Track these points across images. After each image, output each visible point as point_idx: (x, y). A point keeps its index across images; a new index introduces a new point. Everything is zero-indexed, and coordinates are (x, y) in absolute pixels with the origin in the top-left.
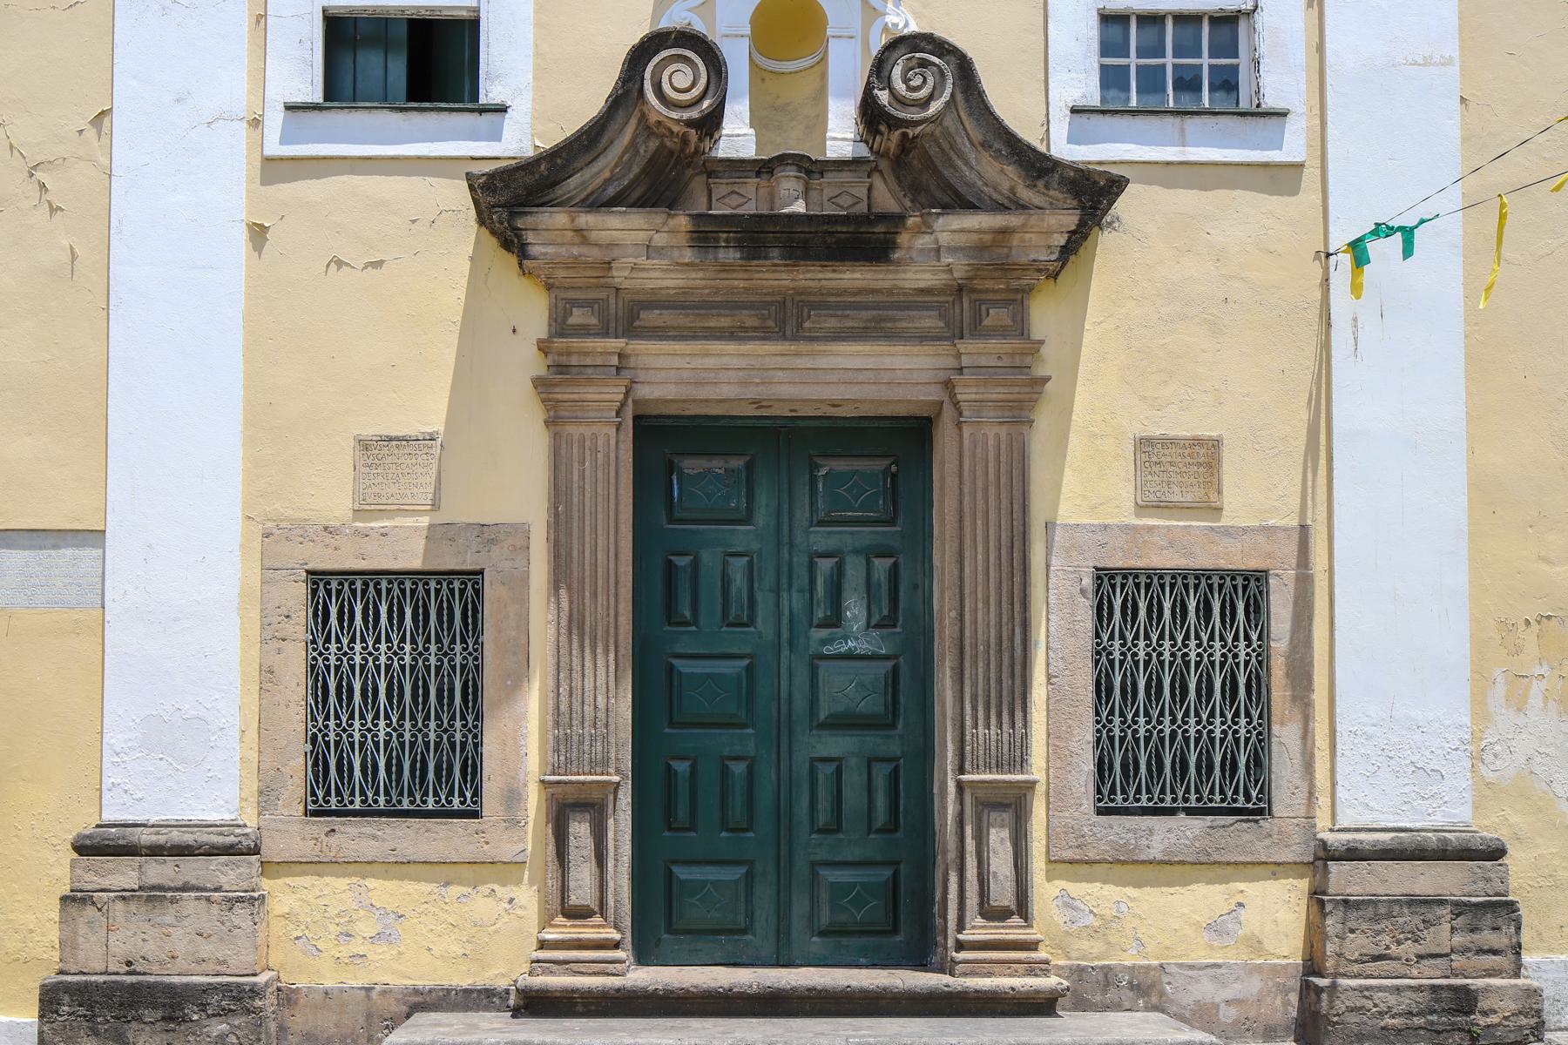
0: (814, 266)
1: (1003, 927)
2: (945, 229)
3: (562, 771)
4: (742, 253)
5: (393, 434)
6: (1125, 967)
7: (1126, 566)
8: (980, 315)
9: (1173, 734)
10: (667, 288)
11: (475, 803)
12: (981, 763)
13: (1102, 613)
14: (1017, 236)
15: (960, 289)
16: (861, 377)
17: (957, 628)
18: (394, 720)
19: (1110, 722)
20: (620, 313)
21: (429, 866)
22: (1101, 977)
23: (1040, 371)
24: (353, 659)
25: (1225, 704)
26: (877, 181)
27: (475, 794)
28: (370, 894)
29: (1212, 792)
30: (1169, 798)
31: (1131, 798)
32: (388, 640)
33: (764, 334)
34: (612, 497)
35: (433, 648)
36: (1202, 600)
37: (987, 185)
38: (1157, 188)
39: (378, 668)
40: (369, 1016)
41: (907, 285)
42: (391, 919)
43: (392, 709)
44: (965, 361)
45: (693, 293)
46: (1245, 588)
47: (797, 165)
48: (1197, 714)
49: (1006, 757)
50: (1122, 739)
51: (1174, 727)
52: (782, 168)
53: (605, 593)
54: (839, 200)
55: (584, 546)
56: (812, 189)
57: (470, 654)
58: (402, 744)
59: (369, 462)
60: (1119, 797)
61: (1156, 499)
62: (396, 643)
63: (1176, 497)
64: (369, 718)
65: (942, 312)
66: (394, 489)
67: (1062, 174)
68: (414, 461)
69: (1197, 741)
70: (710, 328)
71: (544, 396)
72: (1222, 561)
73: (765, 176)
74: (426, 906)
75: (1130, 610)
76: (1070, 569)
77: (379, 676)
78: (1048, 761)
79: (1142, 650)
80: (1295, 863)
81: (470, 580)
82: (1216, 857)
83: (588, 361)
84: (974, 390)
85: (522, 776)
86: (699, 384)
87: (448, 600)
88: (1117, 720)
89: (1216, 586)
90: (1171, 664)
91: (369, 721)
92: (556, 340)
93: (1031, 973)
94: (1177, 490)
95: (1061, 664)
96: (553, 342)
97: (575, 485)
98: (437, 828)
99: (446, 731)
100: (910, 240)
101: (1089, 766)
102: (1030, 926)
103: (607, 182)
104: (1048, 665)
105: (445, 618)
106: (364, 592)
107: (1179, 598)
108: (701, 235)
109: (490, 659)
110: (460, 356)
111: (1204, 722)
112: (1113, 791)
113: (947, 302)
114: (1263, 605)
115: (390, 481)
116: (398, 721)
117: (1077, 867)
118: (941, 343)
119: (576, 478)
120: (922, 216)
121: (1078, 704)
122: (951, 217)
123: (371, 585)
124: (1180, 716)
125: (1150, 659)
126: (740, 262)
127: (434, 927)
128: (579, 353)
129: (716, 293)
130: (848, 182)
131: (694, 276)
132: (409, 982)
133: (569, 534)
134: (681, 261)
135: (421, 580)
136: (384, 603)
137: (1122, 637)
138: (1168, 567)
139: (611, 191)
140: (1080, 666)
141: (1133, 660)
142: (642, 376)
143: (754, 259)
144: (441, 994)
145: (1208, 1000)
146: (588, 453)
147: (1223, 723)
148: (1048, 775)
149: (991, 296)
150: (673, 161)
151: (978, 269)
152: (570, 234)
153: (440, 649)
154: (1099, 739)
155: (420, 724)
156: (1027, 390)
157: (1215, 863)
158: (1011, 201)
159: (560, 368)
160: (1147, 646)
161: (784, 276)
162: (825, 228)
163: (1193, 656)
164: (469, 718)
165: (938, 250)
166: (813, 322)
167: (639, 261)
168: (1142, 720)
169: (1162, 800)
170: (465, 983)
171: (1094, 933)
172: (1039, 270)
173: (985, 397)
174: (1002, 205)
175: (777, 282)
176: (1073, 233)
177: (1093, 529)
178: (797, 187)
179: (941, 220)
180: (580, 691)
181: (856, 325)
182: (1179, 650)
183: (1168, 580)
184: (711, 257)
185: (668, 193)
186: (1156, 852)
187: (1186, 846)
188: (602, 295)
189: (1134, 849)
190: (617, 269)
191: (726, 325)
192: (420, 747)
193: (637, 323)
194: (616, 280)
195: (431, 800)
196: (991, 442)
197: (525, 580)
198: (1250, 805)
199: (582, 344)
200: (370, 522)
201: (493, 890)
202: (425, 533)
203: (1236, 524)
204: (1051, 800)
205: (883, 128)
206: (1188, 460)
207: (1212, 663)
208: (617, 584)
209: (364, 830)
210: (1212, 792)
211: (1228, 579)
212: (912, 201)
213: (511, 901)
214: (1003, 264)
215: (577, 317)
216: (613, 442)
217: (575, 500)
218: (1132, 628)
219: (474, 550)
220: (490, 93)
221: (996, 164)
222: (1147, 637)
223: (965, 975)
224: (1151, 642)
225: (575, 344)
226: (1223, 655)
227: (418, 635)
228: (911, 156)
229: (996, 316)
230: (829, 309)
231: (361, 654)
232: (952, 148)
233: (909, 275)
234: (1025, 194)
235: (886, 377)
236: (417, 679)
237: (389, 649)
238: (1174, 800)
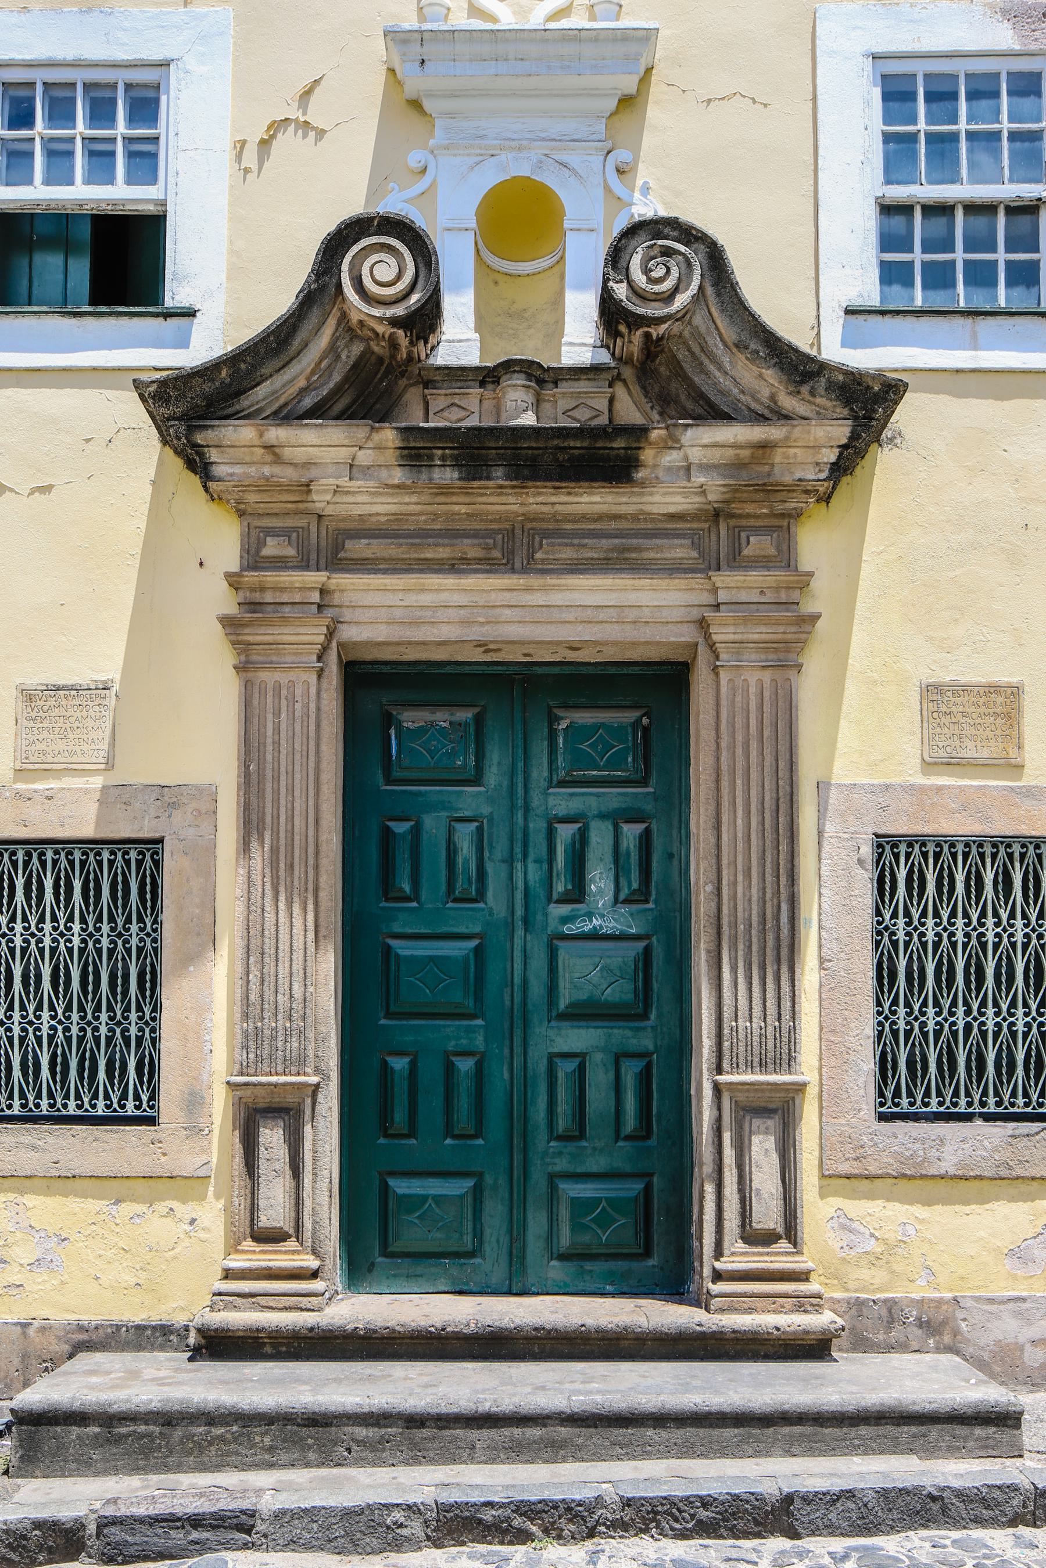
0: (546, 487)
1: (768, 1254)
2: (695, 443)
3: (252, 1071)
4: (461, 472)
5: (61, 682)
6: (913, 1300)
7: (911, 832)
8: (740, 544)
9: (968, 1027)
10: (378, 514)
11: (152, 1107)
12: (741, 1061)
13: (884, 886)
14: (779, 450)
15: (717, 514)
16: (602, 615)
17: (713, 905)
18: (60, 1012)
19: (894, 1013)
20: (323, 543)
21: (98, 1182)
22: (884, 1312)
23: (808, 607)
24: (12, 941)
25: (1029, 992)
26: (620, 390)
27: (152, 1098)
28: (29, 1213)
29: (1014, 1094)
30: (963, 1101)
31: (919, 1102)
32: (54, 918)
33: (489, 565)
34: (312, 753)
35: (105, 928)
36: (1000, 871)
37: (743, 392)
38: (944, 399)
39: (41, 951)
40: (25, 1356)
41: (655, 509)
42: (53, 1243)
43: (58, 999)
44: (722, 596)
45: (407, 520)
47: (526, 373)
48: (996, 1004)
49: (771, 1055)
50: (908, 1033)
51: (969, 1019)
52: (508, 376)
53: (303, 865)
54: (575, 413)
55: (278, 809)
56: (545, 401)
57: (148, 935)
58: (68, 1039)
59: (34, 714)
60: (905, 1101)
61: (946, 755)
62: (62, 922)
63: (969, 751)
64: (31, 1009)
65: (696, 541)
66: (61, 746)
67: (829, 378)
68: (85, 714)
69: (996, 1035)
70: (426, 559)
71: (233, 638)
72: (1024, 827)
73: (490, 386)
74: (94, 1227)
75: (916, 883)
76: (845, 836)
77: (43, 960)
78: (821, 1059)
79: (930, 929)
81: (148, 850)
82: (1019, 1171)
83: (285, 598)
84: (731, 629)
85: (205, 1077)
86: (415, 623)
87: (123, 873)
88: (902, 1011)
89: (1017, 855)
90: (965, 945)
91: (31, 1012)
92: (246, 573)
93: (800, 1309)
94: (970, 744)
95: (835, 946)
96: (243, 576)
97: (269, 741)
98: (107, 1136)
99: (119, 1024)
100: (655, 457)
101: (869, 1065)
102: (800, 1253)
103: (303, 392)
104: (820, 946)
105: (120, 894)
106: (26, 864)
107: (973, 869)
108: (413, 452)
109: (170, 940)
110: (140, 593)
111: (1004, 1014)
112: (897, 1094)
113: (703, 530)
115: (57, 736)
116: (64, 1013)
118: (694, 575)
119: (270, 732)
120: (667, 428)
121: (855, 992)
122: (701, 429)
123: (35, 855)
124: (975, 1007)
125: (940, 940)
126: (459, 483)
127: (102, 1252)
128: (274, 589)
129: (433, 520)
130: (586, 393)
131: (407, 499)
132: (72, 1317)
133: (261, 795)
134: (390, 482)
135: (92, 850)
136: (49, 874)
137: (907, 914)
138: (960, 833)
139: (308, 402)
140: (858, 948)
141: (920, 940)
142: (347, 615)
143: (474, 479)
144: (109, 1330)
145: (1011, 1340)
146: (284, 703)
147: (1026, 1015)
148: (821, 1075)
149: (752, 522)
150: (383, 369)
151: (736, 491)
152: (262, 451)
153: (113, 929)
154: (880, 1034)
155: (89, 1017)
156: (793, 629)
158: (772, 411)
159: (252, 606)
160: (937, 925)
161: (512, 499)
162: (556, 442)
163: (990, 937)
164: (146, 1010)
165: (688, 468)
166: (547, 553)
167: (340, 482)
168: (931, 1011)
169: (955, 1105)
170: (138, 1319)
171: (875, 1260)
172: (807, 492)
173: (745, 637)
174: (762, 416)
175: (503, 507)
176: (844, 447)
177: (872, 790)
178: (525, 398)
179: (690, 433)
180: (273, 978)
181: (596, 556)
182: (975, 929)
184: (424, 476)
185: (378, 406)
186: (948, 1166)
188: (300, 522)
189: (923, 1161)
190: (318, 491)
191: (445, 556)
192: (90, 1043)
193: (341, 555)
194: (318, 505)
195: (101, 1103)
196: (752, 690)
197: (211, 849)
199: (277, 579)
200: (33, 783)
201: (171, 1209)
202: (97, 795)
203: (1039, 784)
204: (824, 1104)
205: (622, 328)
206: (983, 709)
207: (1013, 945)
208: (317, 853)
209: (22, 1139)
210: (1014, 1094)
211: (1031, 848)
212: (661, 414)
213: (193, 1221)
214: (764, 485)
215: (272, 548)
216: (313, 691)
217: (269, 757)
218: (919, 905)
219: (153, 814)
220: (175, 295)
221: (754, 368)
222: (937, 914)
223: (721, 1310)
224: (941, 919)
225: (268, 579)
227: (89, 914)
228: (657, 362)
229: (758, 545)
230: (564, 538)
231: (22, 935)
232: (702, 350)
233: (657, 498)
234: (788, 402)
235: (631, 615)
236: (86, 964)
237: (55, 929)
238: (970, 1104)
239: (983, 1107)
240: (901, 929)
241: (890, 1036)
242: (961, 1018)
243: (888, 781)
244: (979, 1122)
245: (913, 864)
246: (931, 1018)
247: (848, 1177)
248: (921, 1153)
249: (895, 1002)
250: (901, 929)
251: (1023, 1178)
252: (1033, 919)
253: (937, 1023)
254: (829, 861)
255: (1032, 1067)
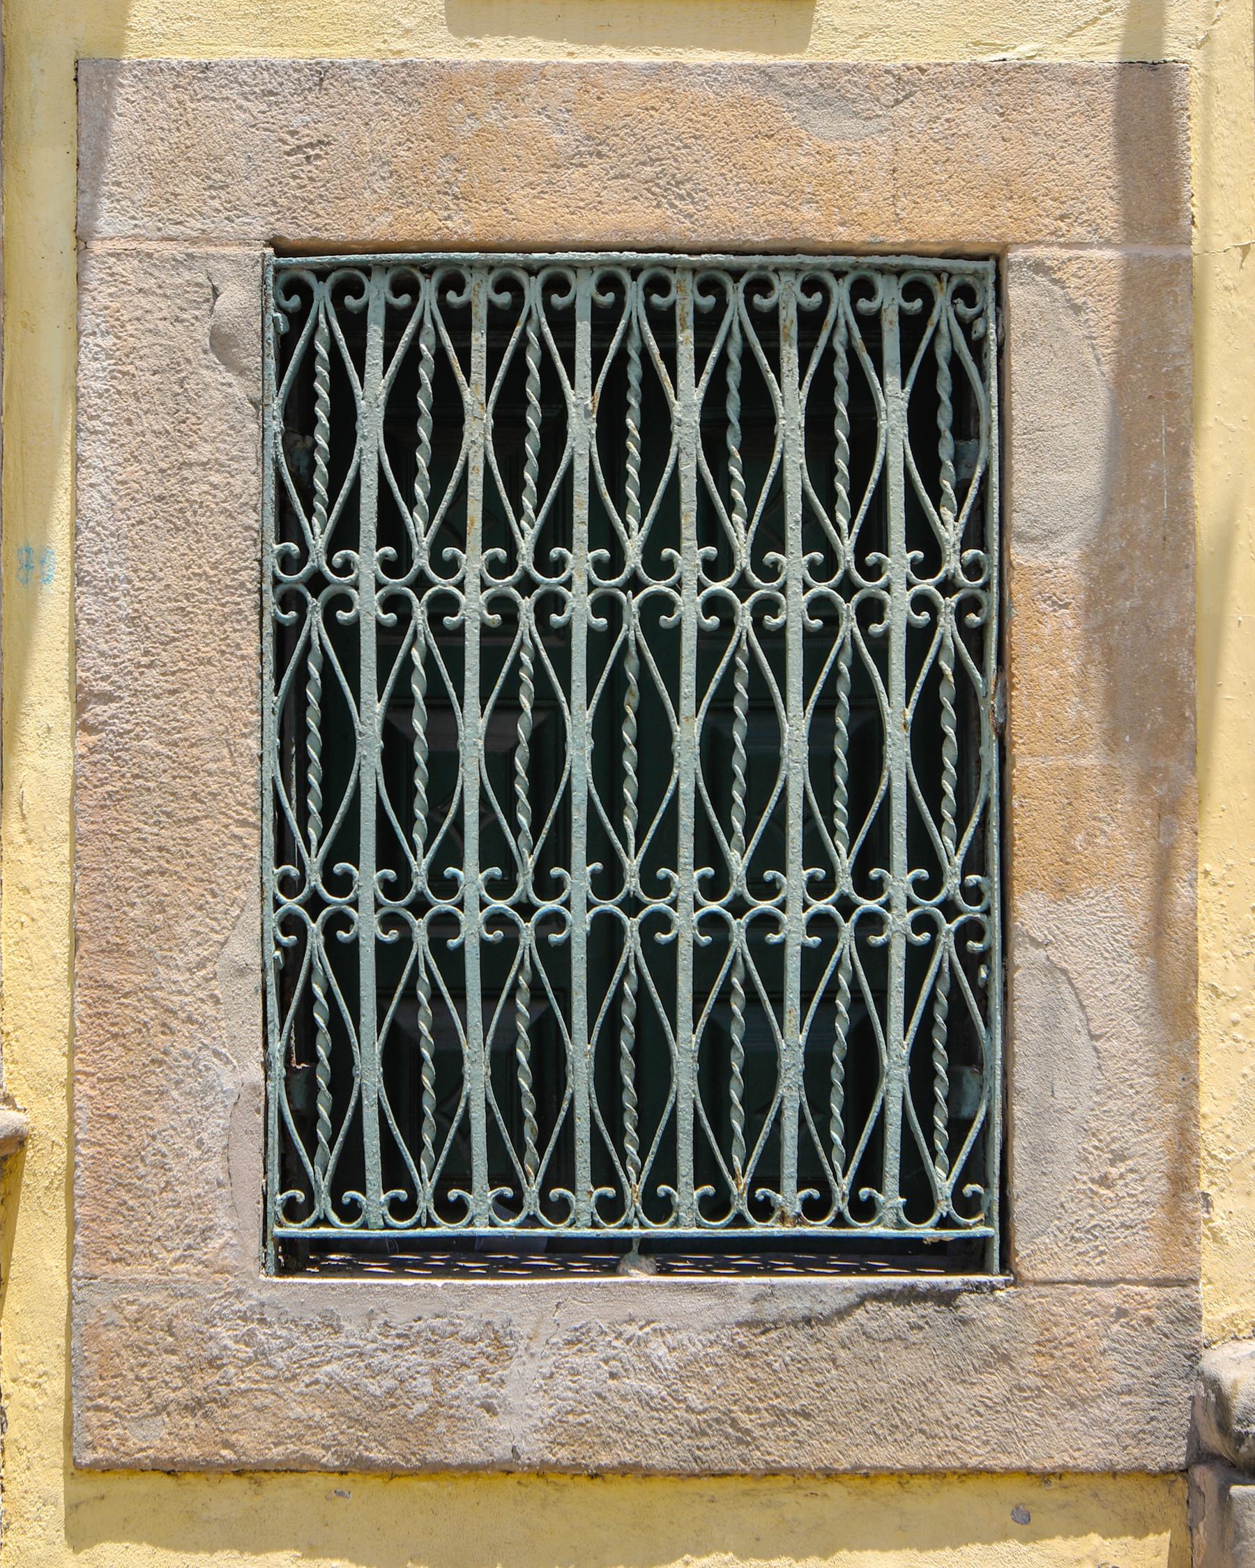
7: (403, 233)
19: (341, 885)
29: (768, 1175)
31: (425, 1202)
46: (912, 327)
48: (709, 852)
51: (609, 906)
72: (808, 212)
76: (169, 249)
78: (73, 1051)
79: (473, 583)
80: (1113, 1473)
82: (776, 1450)
95: (125, 643)
104: (76, 646)
111: (738, 884)
114: (986, 396)
117: (199, 1489)
121: (195, 809)
140: (207, 651)
147: (818, 888)
154: (293, 957)
157: (773, 1472)
160: (498, 569)
169: (560, 1211)
183: (584, 292)
187: (646, 1401)
189: (431, 1416)
198: (926, 1231)
207: (774, 641)
211: (840, 291)
224: (512, 549)
226: (819, 606)
238: (610, 1209)
239: (658, 1217)
240: (367, 584)
241: (324, 965)
242: (578, 903)
243: (327, 55)
244: (639, 1275)
245: (413, 354)
246: (472, 903)
247: (172, 1470)
248: (424, 1385)
249: (346, 847)
250: (367, 584)
251: (791, 1472)
252: (846, 547)
253: (495, 921)
254: (108, 342)
255: (837, 1074)
